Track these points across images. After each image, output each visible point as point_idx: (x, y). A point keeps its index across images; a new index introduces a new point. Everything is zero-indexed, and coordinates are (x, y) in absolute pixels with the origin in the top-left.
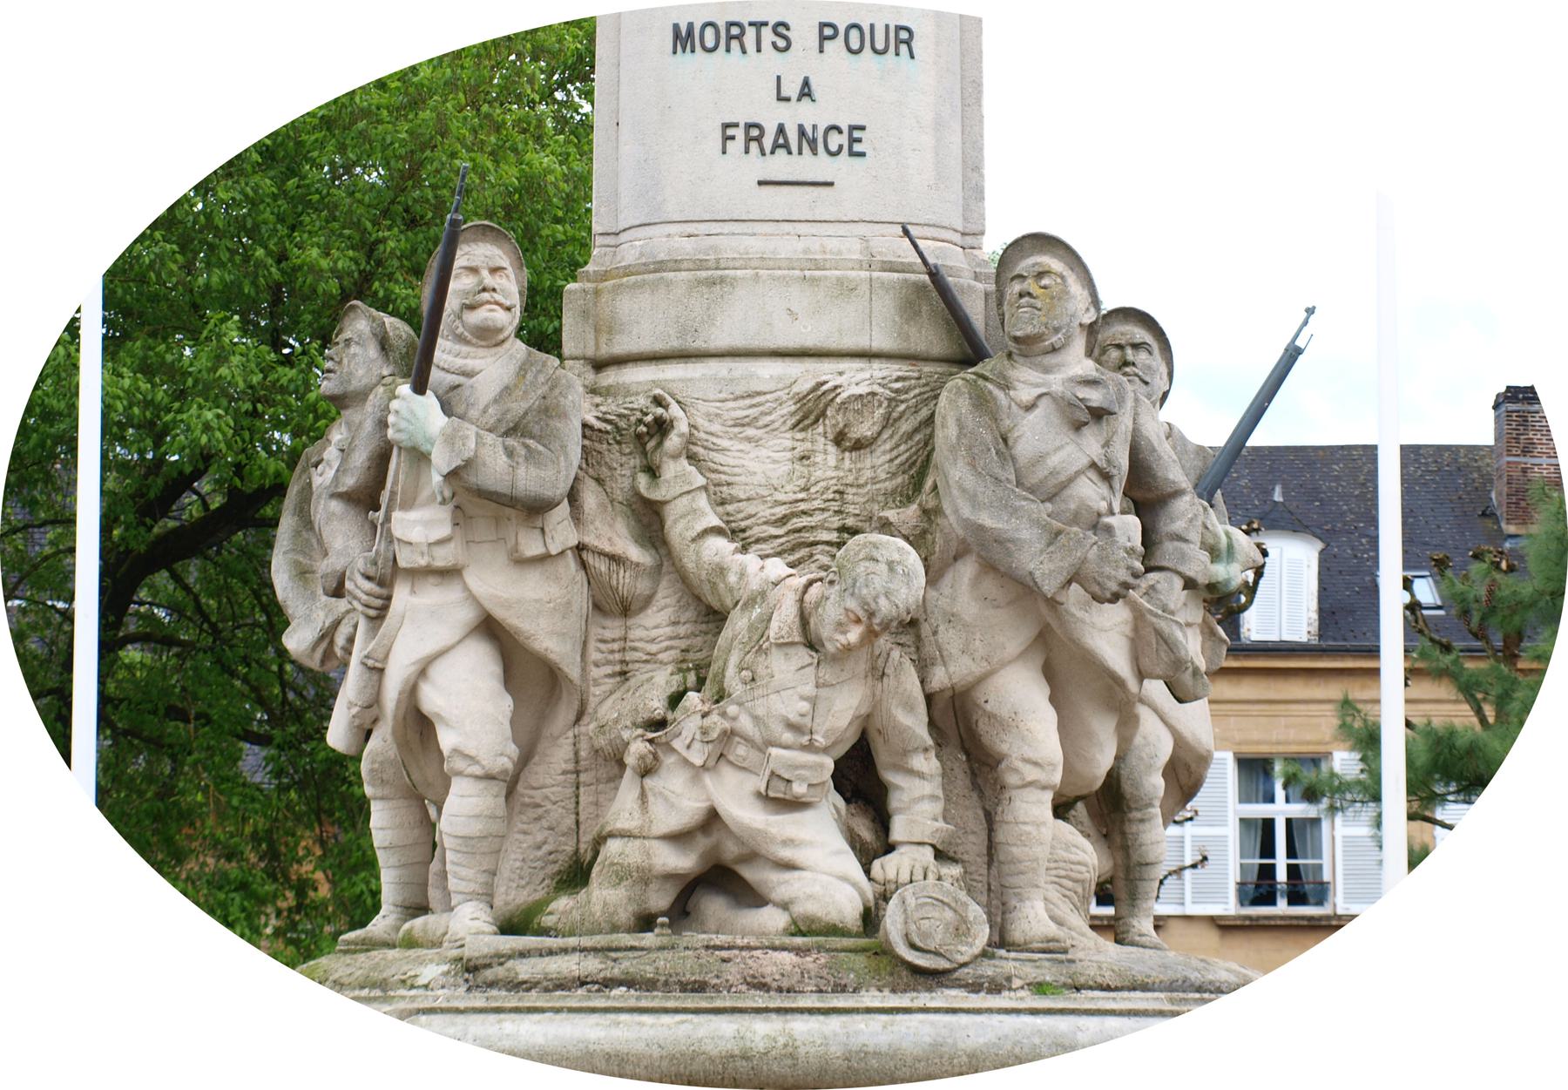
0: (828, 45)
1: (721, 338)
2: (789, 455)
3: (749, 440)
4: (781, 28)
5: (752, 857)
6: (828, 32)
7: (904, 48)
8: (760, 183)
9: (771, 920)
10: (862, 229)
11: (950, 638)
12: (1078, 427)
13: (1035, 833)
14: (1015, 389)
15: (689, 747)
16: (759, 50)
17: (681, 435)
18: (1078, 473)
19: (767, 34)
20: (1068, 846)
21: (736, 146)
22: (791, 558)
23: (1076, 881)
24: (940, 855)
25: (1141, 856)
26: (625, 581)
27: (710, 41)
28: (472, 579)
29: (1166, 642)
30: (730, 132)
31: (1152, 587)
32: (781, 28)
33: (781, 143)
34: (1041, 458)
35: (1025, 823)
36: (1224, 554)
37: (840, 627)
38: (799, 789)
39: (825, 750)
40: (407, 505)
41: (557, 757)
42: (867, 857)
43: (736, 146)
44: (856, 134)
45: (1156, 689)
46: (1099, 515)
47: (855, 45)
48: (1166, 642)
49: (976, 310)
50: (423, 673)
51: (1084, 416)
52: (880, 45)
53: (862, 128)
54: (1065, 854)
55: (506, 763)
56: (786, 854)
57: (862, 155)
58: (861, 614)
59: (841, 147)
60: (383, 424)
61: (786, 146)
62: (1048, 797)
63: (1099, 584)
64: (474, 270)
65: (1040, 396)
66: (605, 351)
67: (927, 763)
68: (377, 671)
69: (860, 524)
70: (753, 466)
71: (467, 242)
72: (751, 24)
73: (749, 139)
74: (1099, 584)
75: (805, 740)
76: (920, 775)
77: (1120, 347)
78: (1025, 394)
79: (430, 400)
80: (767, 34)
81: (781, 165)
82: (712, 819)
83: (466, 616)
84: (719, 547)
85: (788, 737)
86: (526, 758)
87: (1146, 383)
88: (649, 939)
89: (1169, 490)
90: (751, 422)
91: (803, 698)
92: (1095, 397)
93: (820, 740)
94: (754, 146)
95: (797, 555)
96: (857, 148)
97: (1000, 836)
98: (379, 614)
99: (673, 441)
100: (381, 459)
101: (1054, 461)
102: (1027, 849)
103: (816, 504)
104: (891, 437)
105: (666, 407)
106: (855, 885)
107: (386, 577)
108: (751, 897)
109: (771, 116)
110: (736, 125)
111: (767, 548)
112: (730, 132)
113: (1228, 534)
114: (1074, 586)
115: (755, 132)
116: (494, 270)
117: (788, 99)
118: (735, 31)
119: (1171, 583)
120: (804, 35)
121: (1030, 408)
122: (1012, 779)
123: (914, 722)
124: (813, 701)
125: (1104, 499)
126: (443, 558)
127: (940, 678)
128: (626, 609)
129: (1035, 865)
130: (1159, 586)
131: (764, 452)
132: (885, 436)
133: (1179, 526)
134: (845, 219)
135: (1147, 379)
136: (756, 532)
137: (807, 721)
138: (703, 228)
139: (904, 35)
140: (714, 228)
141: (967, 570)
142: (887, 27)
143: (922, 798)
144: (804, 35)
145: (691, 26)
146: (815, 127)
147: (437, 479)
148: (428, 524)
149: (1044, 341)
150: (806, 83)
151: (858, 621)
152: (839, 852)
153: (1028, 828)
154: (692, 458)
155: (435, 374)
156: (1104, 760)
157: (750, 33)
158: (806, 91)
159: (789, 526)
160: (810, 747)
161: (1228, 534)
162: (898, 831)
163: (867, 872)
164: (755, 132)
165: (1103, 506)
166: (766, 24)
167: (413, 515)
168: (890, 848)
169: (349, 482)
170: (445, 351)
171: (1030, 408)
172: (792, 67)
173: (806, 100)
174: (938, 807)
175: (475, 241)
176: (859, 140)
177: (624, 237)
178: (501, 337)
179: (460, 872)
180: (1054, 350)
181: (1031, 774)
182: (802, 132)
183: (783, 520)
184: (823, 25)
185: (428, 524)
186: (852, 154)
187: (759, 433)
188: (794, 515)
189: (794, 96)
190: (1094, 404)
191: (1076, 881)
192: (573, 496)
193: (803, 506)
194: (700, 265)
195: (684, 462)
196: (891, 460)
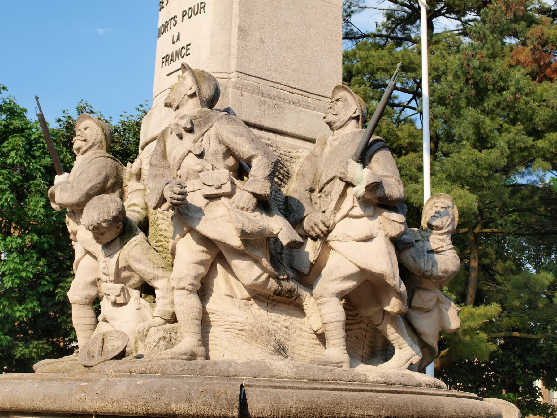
8: (168, 75)
43: (164, 64)
44: (188, 47)
53: (189, 45)
54: (228, 319)
59: (184, 54)
87: (336, 115)
96: (188, 52)
125: (198, 164)
137: (106, 271)
142: (198, 4)
166: (172, 19)
175: (84, 121)
176: (188, 50)
178: (82, 151)
184: (184, 11)
186: (187, 55)
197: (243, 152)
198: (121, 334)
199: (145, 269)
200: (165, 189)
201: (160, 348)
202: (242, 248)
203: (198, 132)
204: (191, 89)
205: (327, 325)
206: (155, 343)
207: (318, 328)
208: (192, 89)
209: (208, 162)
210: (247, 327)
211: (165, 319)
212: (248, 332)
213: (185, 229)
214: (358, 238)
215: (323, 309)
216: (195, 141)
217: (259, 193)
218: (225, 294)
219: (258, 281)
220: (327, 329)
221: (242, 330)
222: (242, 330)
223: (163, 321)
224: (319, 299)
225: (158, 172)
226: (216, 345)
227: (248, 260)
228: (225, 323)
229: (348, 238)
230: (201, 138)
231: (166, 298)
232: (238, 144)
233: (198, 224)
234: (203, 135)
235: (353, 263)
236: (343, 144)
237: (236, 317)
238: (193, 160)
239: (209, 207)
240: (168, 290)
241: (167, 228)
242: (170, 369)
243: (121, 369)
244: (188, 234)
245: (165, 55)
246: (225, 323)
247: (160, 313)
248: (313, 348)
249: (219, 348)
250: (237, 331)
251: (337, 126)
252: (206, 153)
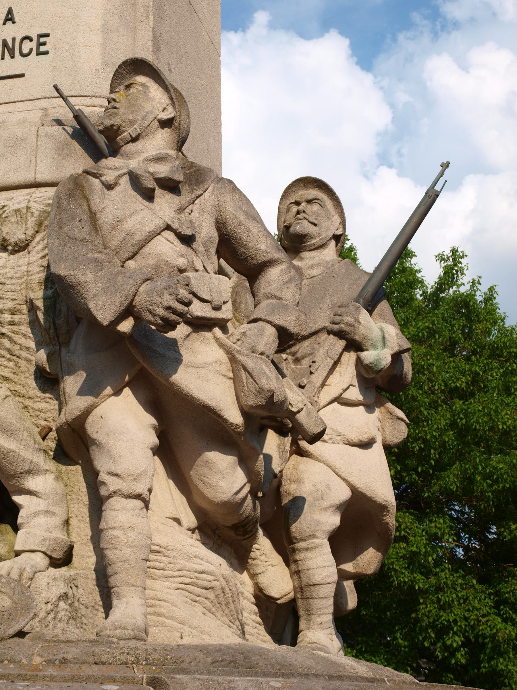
10: (44, 103)
13: (122, 537)
14: (105, 175)
25: (309, 578)
29: (252, 377)
31: (244, 334)
34: (119, 222)
35: (113, 528)
36: (380, 344)
44: (42, 40)
46: (181, 271)
48: (252, 377)
53: (47, 35)
54: (189, 565)
57: (46, 53)
59: (31, 50)
63: (150, 312)
65: (121, 176)
69: (18, 307)
74: (150, 312)
77: (298, 203)
87: (315, 225)
89: (263, 259)
96: (42, 48)
101: (130, 224)
102: (116, 551)
104: (43, 239)
113: (382, 330)
119: (262, 332)
125: (182, 256)
129: (126, 565)
130: (248, 333)
132: (38, 238)
134: (32, 98)
135: (314, 221)
143: (37, 514)
146: (14, 39)
149: (122, 133)
150: (10, 11)
153: (116, 533)
161: (382, 330)
165: (181, 262)
173: (9, 23)
176: (44, 44)
186: (39, 53)
190: (162, 176)
196: (44, 257)
197: (257, 249)
198: (8, 583)
199: (17, 450)
200: (142, 288)
201: (60, 616)
202: (242, 429)
203: (187, 193)
204: (164, 109)
205: (317, 588)
206: (50, 606)
207: (284, 594)
208: (166, 112)
209: (197, 255)
210: (218, 583)
211: (50, 557)
212: (217, 593)
213: (127, 378)
214: (356, 440)
215: (311, 558)
216: (181, 210)
217: (292, 331)
218: (172, 516)
219: (237, 496)
220: (314, 596)
221: (209, 588)
222: (207, 589)
223: (46, 561)
224: (305, 540)
225: (96, 255)
226: (159, 615)
227: (233, 456)
228: (179, 573)
229: (338, 438)
230: (190, 207)
231: (53, 514)
232: (250, 234)
233: (176, 371)
234: (193, 203)
235: (345, 480)
236: (334, 275)
237: (202, 562)
238: (171, 245)
239: (188, 342)
240: (58, 498)
241: (11, 376)
242: (187, 659)
243: (69, 656)
244: (127, 391)
246: (179, 573)
247: (47, 544)
248: (256, 630)
249: (168, 621)
250: (199, 590)
251: (314, 244)
252: (197, 239)
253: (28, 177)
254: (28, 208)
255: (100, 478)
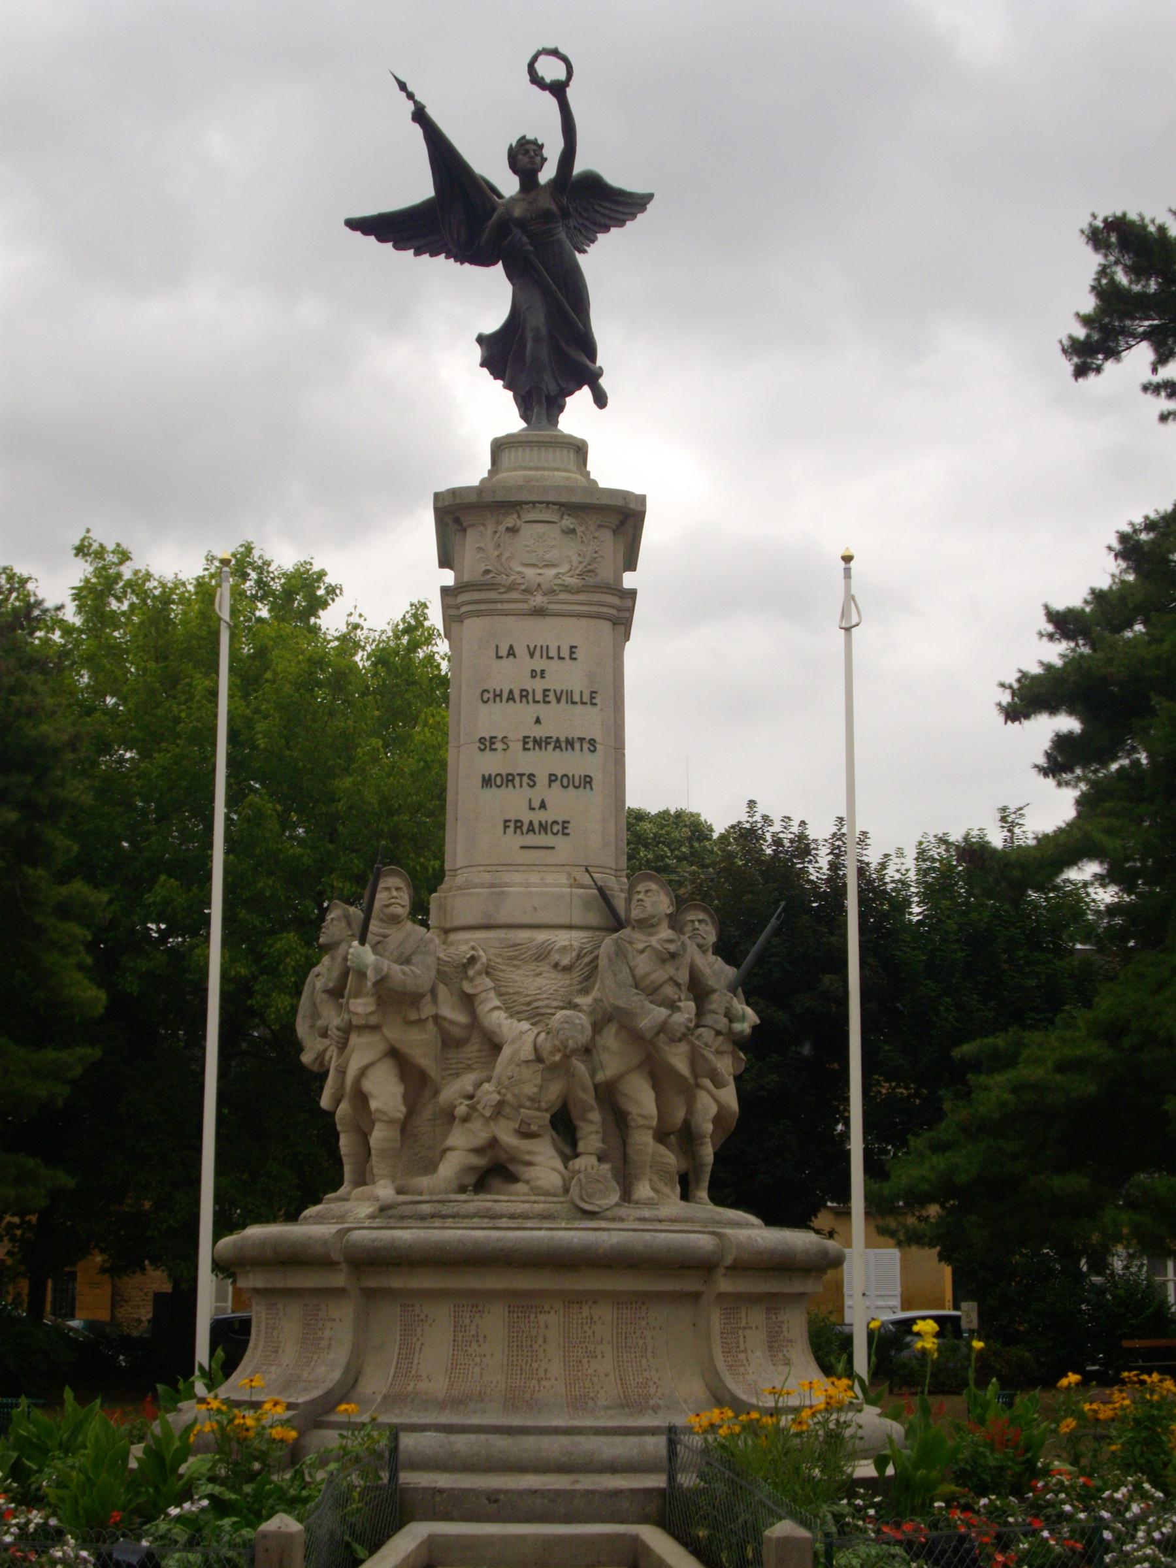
0: (553, 785)
1: (502, 918)
2: (532, 973)
3: (515, 966)
4: (531, 776)
5: (514, 1159)
6: (553, 778)
7: (588, 786)
8: (522, 847)
9: (521, 1187)
10: (567, 869)
11: (605, 1057)
12: (664, 961)
15: (484, 1108)
16: (521, 786)
17: (483, 964)
18: (664, 983)
19: (525, 779)
20: (662, 1156)
21: (510, 830)
22: (533, 1021)
23: (666, 1172)
24: (600, 1159)
26: (457, 1032)
27: (499, 782)
28: (386, 1031)
30: (508, 824)
31: (700, 1035)
32: (531, 776)
33: (531, 829)
34: (648, 975)
37: (552, 1053)
38: (534, 1128)
39: (546, 1110)
40: (357, 995)
41: (427, 1113)
42: (566, 1159)
43: (510, 830)
44: (566, 825)
45: (707, 1082)
47: (565, 783)
49: (620, 904)
50: (363, 1072)
51: (667, 956)
52: (577, 784)
55: (400, 1116)
56: (528, 1158)
58: (561, 1047)
59: (558, 831)
60: (345, 959)
61: (533, 831)
62: (650, 1133)
64: (388, 889)
66: (448, 925)
67: (595, 1116)
68: (342, 1072)
70: (518, 978)
71: (386, 876)
72: (518, 774)
73: (516, 828)
75: (536, 1105)
76: (591, 1122)
78: (640, 946)
79: (367, 947)
80: (525, 779)
81: (531, 840)
82: (494, 1143)
83: (381, 1047)
84: (502, 1015)
85: (528, 1104)
86: (411, 1112)
88: (463, 1197)
90: (516, 958)
91: (535, 1086)
92: (672, 948)
93: (543, 1105)
94: (518, 831)
95: (536, 1019)
96: (566, 831)
97: (630, 1150)
98: (343, 1046)
99: (478, 966)
100: (345, 974)
101: (654, 976)
103: (545, 996)
105: (476, 951)
106: (560, 1173)
107: (348, 1030)
108: (513, 1178)
109: (526, 817)
110: (510, 821)
111: (522, 1016)
112: (508, 824)
114: (662, 1035)
115: (519, 824)
116: (397, 889)
117: (534, 809)
118: (510, 778)
120: (542, 780)
121: (642, 952)
122: (633, 1124)
123: (589, 1098)
124: (541, 1087)
126: (373, 1020)
127: (600, 1077)
128: (460, 1043)
131: (521, 972)
133: (714, 1006)
136: (517, 1008)
138: (494, 868)
139: (588, 779)
140: (500, 868)
141: (612, 1029)
142: (580, 777)
143: (592, 1133)
144: (542, 780)
145: (490, 775)
147: (369, 984)
148: (364, 1005)
151: (560, 1051)
152: (553, 1157)
154: (488, 974)
155: (370, 936)
156: (680, 1115)
157: (517, 779)
158: (543, 805)
159: (532, 1006)
160: (538, 1109)
161: (743, 1009)
162: (581, 1147)
163: (566, 1167)
164: (519, 824)
166: (524, 774)
167: (359, 1001)
168: (577, 1155)
169: (331, 985)
170: (374, 926)
171: (642, 952)
172: (536, 795)
173: (542, 810)
174: (599, 1137)
176: (567, 828)
177: (459, 872)
179: (377, 1164)
180: (653, 926)
181: (641, 1122)
182: (540, 823)
183: (529, 1004)
184: (551, 775)
185: (364, 1005)
186: (565, 834)
187: (519, 963)
188: (536, 1001)
189: (537, 807)
191: (666, 1172)
192: (433, 992)
193: (538, 997)
194: (492, 886)
195: (484, 976)
245: (513, 819)
253: (567, 921)
254: (571, 945)
255: (629, 1117)
